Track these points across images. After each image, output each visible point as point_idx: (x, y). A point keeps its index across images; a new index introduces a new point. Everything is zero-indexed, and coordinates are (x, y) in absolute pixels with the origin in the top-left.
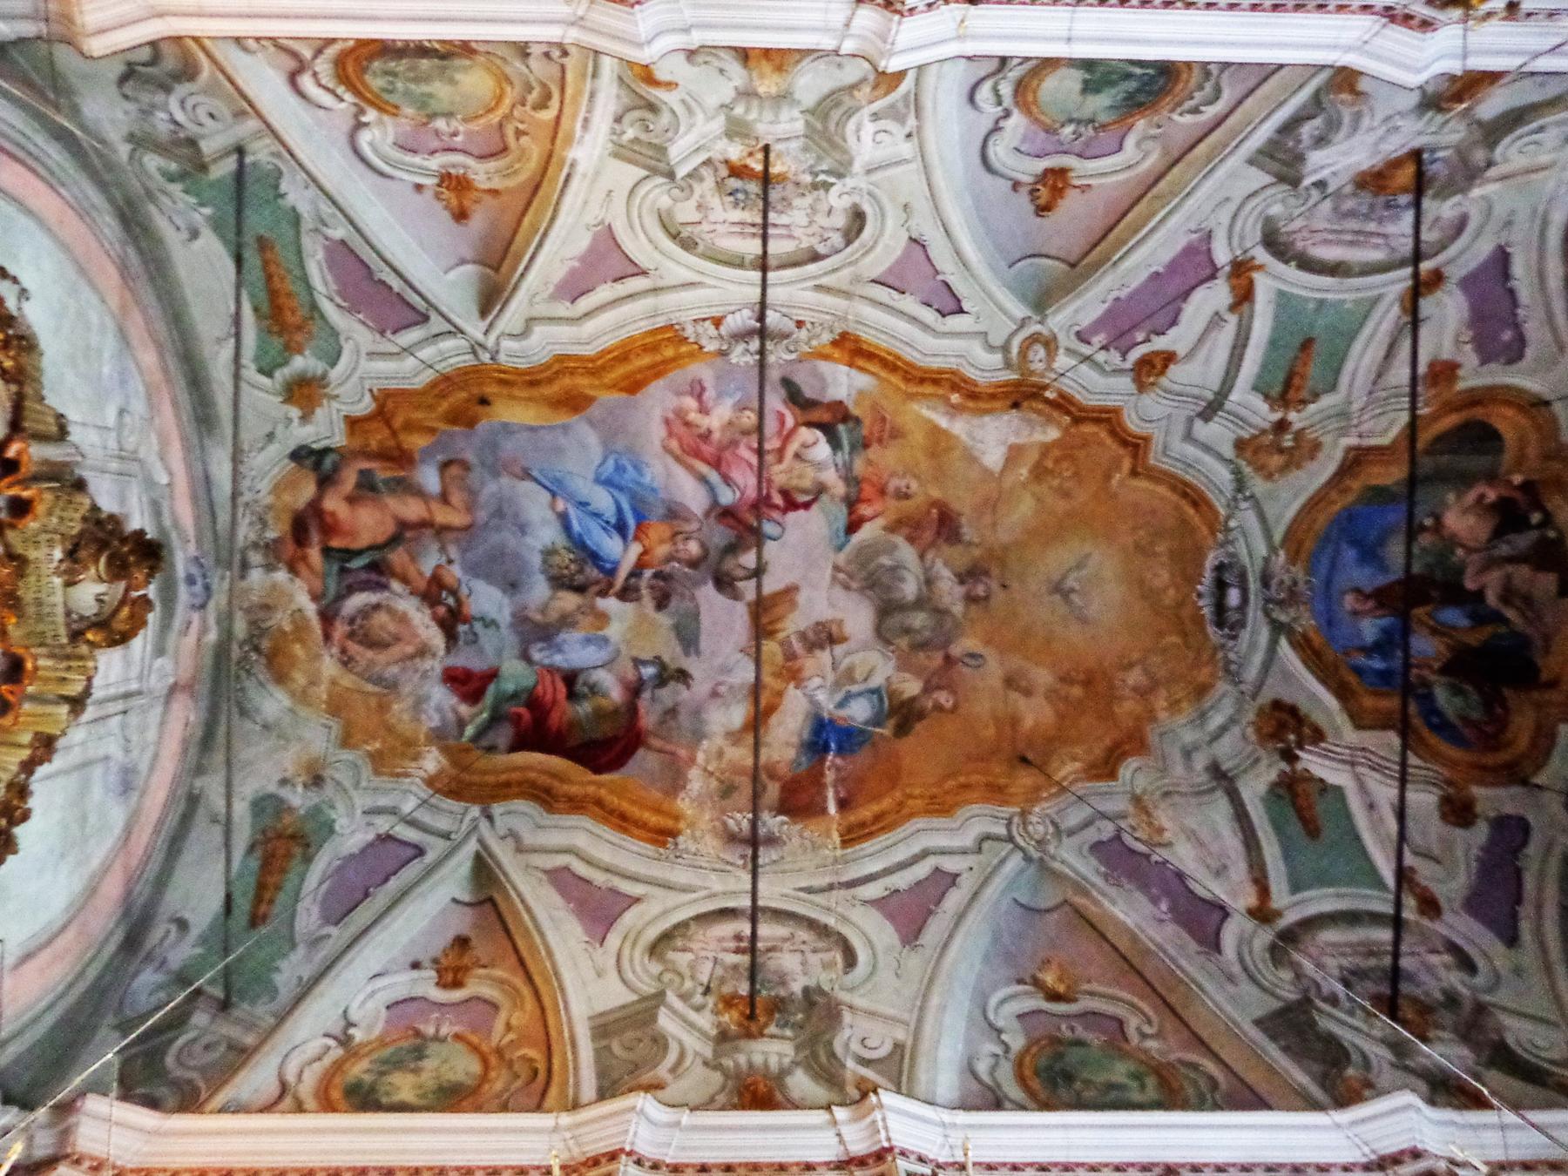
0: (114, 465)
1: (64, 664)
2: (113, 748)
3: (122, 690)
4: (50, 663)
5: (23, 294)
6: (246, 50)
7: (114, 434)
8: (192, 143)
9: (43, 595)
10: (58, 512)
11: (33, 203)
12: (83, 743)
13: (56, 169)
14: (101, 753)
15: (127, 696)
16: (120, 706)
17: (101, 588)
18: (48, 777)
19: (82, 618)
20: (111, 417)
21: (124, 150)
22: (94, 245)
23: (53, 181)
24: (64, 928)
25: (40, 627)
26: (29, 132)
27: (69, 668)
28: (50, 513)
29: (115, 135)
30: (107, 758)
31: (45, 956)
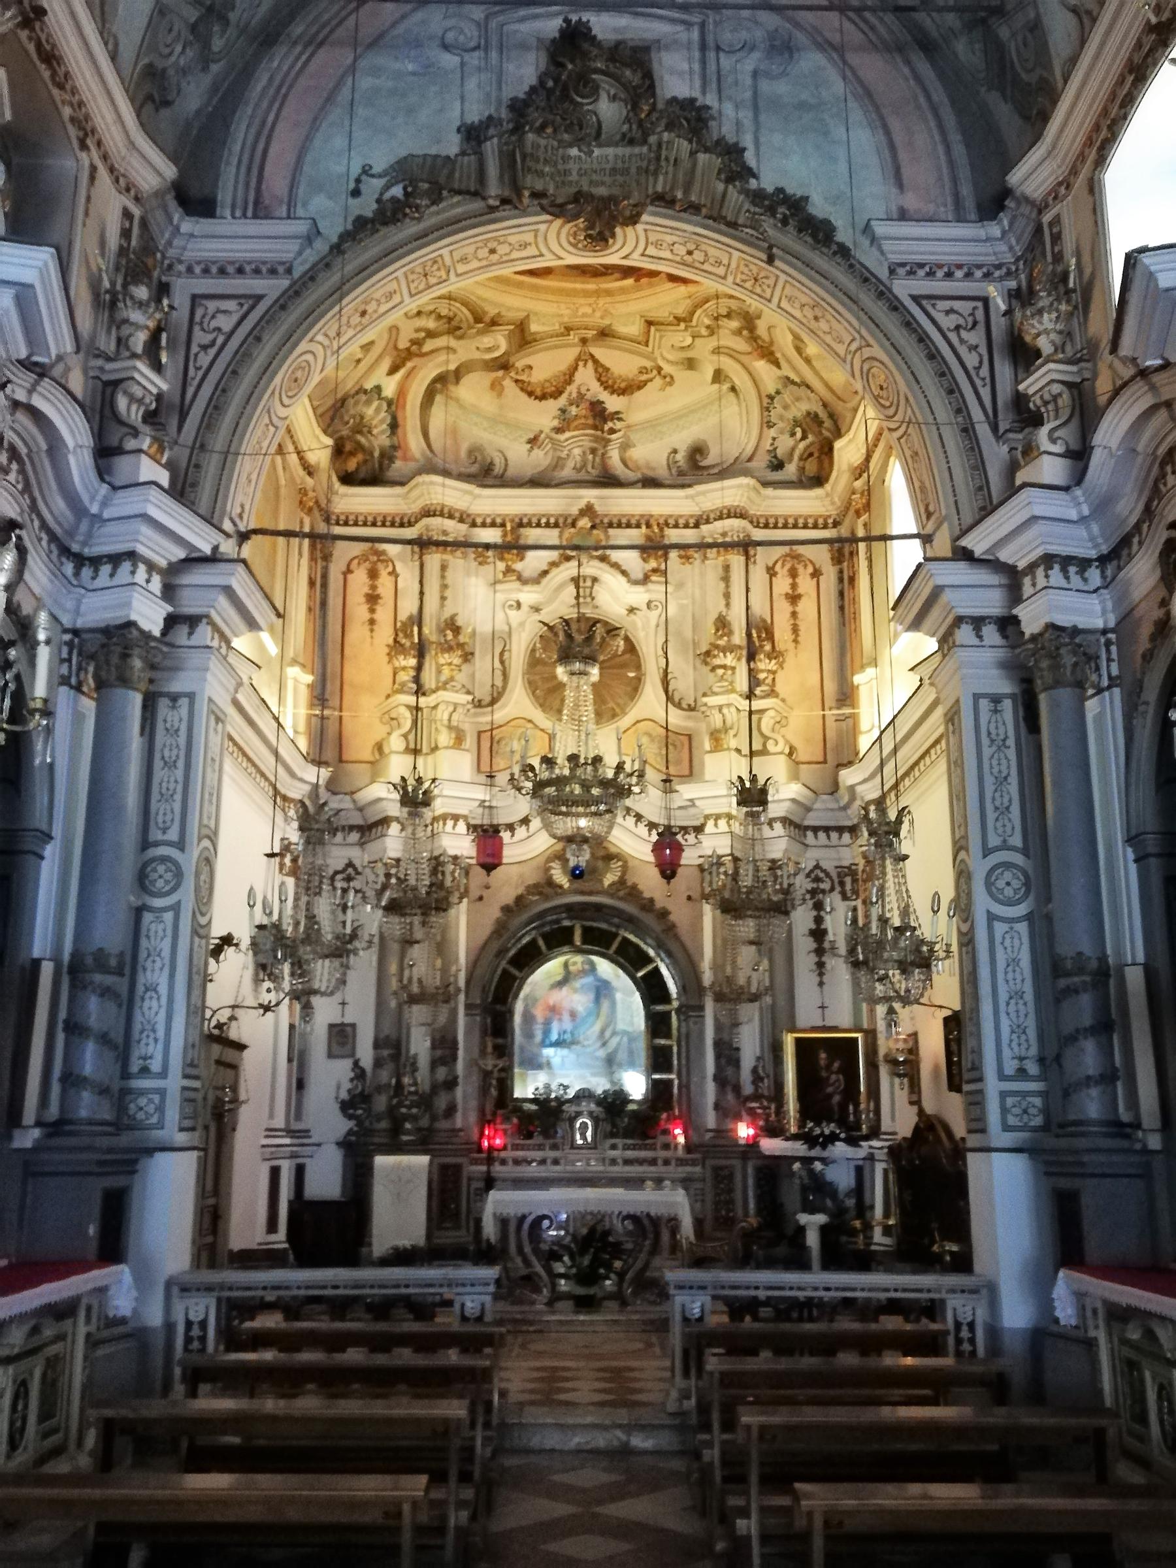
0: (494, 54)
1: (663, 163)
2: (750, 63)
3: (697, 54)
4: (661, 178)
5: (366, 171)
6: (116, 45)
7: (467, 57)
8: (194, 28)
9: (609, 166)
10: (540, 167)
11: (291, 158)
12: (737, 107)
13: (253, 131)
14: (749, 81)
15: (703, 47)
16: (711, 55)
17: (604, 96)
18: (757, 154)
19: (627, 120)
20: (449, 60)
21: (215, 68)
22: (303, 82)
23: (265, 135)
24: (887, 133)
25: (633, 170)
26: (235, 161)
27: (667, 159)
28: (540, 174)
29: (206, 80)
30: (755, 74)
31: (903, 156)
